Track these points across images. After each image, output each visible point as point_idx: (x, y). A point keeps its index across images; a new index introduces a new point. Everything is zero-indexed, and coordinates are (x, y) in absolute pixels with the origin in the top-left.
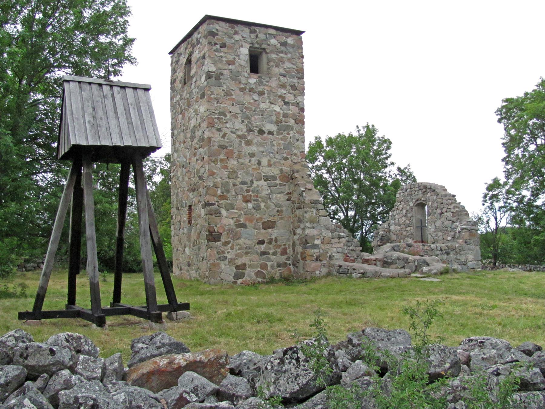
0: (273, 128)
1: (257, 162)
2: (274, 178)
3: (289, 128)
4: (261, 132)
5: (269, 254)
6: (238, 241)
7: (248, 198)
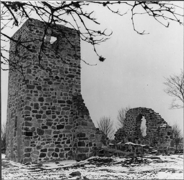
3: (72, 76)
5: (60, 143)
7: (49, 112)
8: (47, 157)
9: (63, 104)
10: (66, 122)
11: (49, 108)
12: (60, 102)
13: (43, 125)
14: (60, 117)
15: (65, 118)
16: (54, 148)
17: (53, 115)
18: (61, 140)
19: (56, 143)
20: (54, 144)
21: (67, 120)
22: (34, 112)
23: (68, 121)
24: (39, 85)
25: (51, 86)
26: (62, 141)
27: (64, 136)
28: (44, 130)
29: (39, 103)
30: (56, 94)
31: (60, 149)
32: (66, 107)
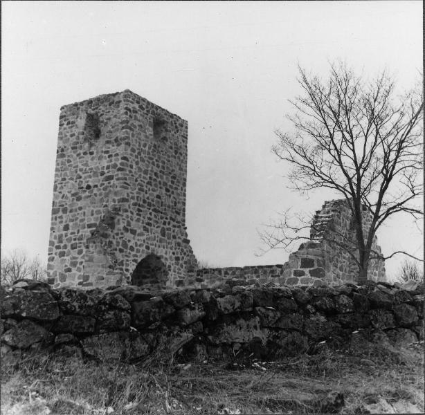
4: (89, 187)
11: (75, 239)
13: (66, 266)
28: (67, 274)
29: (64, 233)
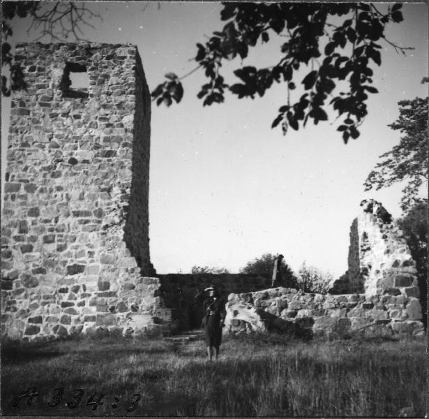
0: (90, 155)
1: (64, 196)
2: (87, 214)
5: (73, 304)
6: (32, 289)
7: (51, 239)
8: (41, 335)
9: (87, 218)
10: (90, 259)
11: (52, 230)
12: (77, 214)
14: (76, 248)
15: (87, 250)
16: (60, 316)
17: (60, 243)
18: (76, 299)
19: (64, 305)
20: (60, 306)
21: (91, 254)
22: (17, 239)
23: (95, 256)
24: (30, 182)
25: (58, 182)
26: (79, 300)
27: (85, 289)
28: (38, 276)
30: (68, 198)
31: (74, 317)
32: (91, 224)
